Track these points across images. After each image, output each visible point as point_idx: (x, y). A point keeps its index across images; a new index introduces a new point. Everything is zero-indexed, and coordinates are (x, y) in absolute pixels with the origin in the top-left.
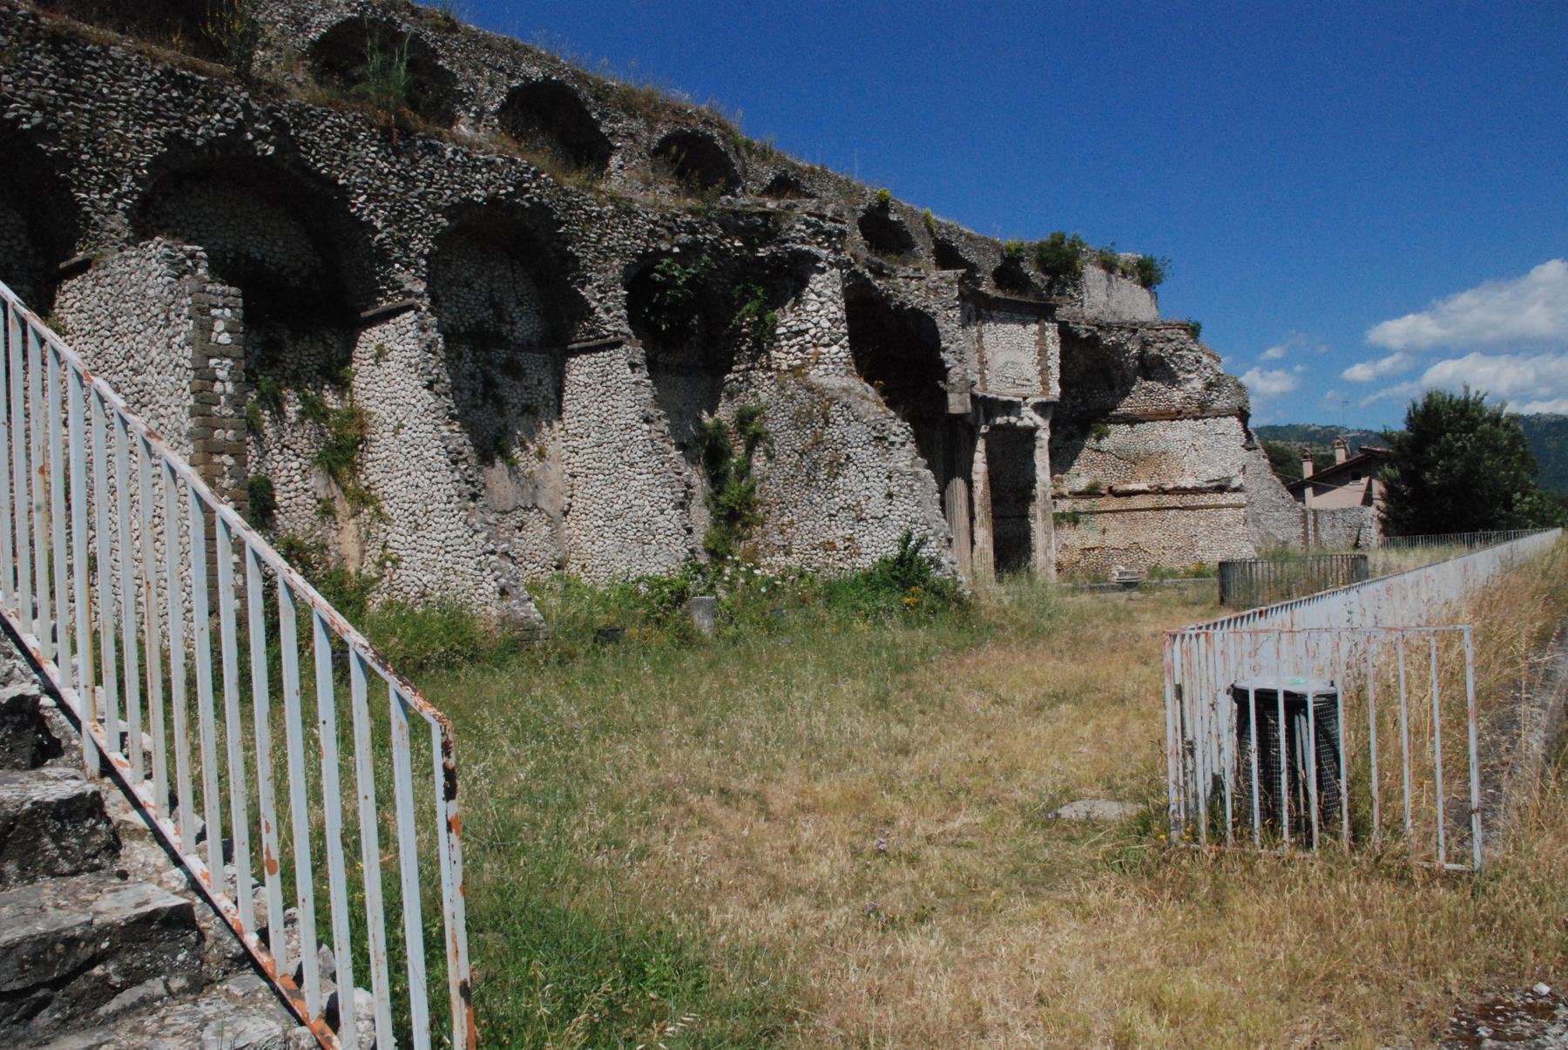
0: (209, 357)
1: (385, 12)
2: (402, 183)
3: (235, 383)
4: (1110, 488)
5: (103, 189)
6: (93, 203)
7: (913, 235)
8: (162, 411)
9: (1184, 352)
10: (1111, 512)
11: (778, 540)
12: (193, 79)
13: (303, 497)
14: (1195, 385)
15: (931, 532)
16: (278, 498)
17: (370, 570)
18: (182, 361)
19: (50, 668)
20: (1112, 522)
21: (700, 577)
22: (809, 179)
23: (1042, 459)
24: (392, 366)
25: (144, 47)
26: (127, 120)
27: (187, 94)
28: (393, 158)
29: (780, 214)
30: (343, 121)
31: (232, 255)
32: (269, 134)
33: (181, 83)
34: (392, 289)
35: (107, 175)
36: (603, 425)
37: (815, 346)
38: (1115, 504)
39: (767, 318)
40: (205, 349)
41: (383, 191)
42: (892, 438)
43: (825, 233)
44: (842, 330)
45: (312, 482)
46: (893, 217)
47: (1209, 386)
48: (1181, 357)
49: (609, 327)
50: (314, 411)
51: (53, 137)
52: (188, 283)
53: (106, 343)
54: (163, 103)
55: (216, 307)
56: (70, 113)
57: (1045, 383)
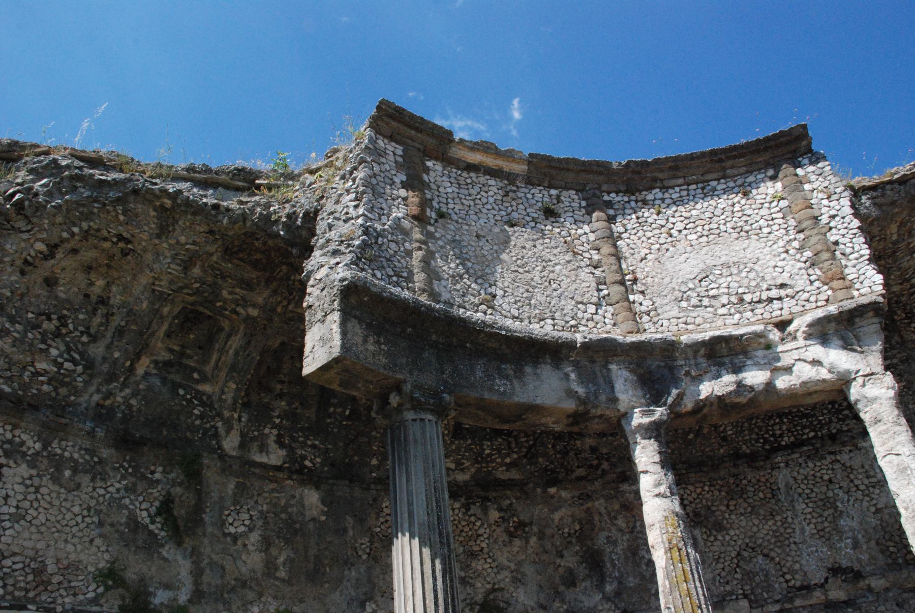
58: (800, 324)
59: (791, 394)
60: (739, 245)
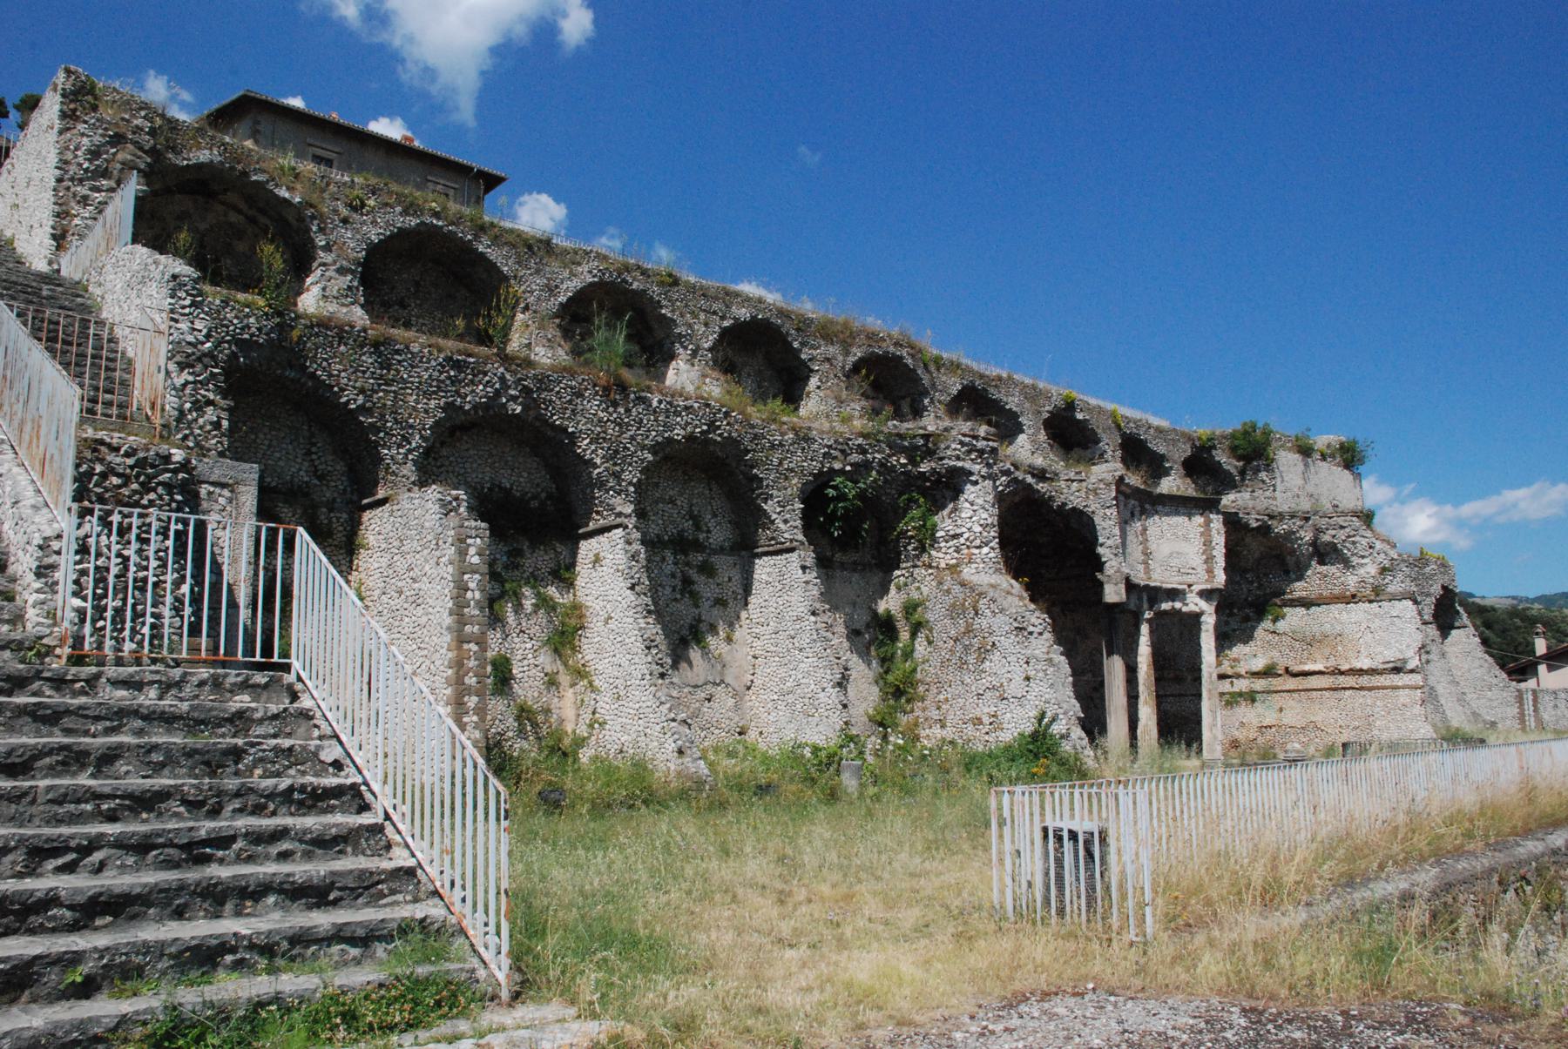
1: (619, 275)
3: (482, 591)
4: (1287, 669)
5: (400, 446)
6: (392, 458)
7: (1099, 431)
9: (1357, 539)
10: (1289, 691)
11: (935, 714)
12: (465, 361)
14: (1369, 569)
15: (1061, 711)
17: (583, 731)
19: (365, 772)
20: (1289, 702)
21: (852, 745)
22: (996, 386)
23: (1207, 641)
24: (605, 570)
25: (433, 340)
26: (418, 395)
27: (460, 372)
28: (611, 409)
29: (939, 435)
32: (517, 397)
33: (459, 366)
35: (403, 436)
36: (779, 616)
37: (968, 547)
38: (1292, 683)
39: (929, 524)
40: (463, 569)
41: (602, 435)
42: (1031, 629)
43: (977, 451)
44: (992, 534)
45: (541, 659)
46: (1080, 416)
47: (1383, 570)
48: (1354, 543)
49: (786, 535)
50: (544, 603)
51: (367, 411)
52: (453, 520)
53: (396, 558)
54: (443, 382)
57: (1210, 571)
58: (1196, 588)
59: (1185, 613)
60: (1183, 544)
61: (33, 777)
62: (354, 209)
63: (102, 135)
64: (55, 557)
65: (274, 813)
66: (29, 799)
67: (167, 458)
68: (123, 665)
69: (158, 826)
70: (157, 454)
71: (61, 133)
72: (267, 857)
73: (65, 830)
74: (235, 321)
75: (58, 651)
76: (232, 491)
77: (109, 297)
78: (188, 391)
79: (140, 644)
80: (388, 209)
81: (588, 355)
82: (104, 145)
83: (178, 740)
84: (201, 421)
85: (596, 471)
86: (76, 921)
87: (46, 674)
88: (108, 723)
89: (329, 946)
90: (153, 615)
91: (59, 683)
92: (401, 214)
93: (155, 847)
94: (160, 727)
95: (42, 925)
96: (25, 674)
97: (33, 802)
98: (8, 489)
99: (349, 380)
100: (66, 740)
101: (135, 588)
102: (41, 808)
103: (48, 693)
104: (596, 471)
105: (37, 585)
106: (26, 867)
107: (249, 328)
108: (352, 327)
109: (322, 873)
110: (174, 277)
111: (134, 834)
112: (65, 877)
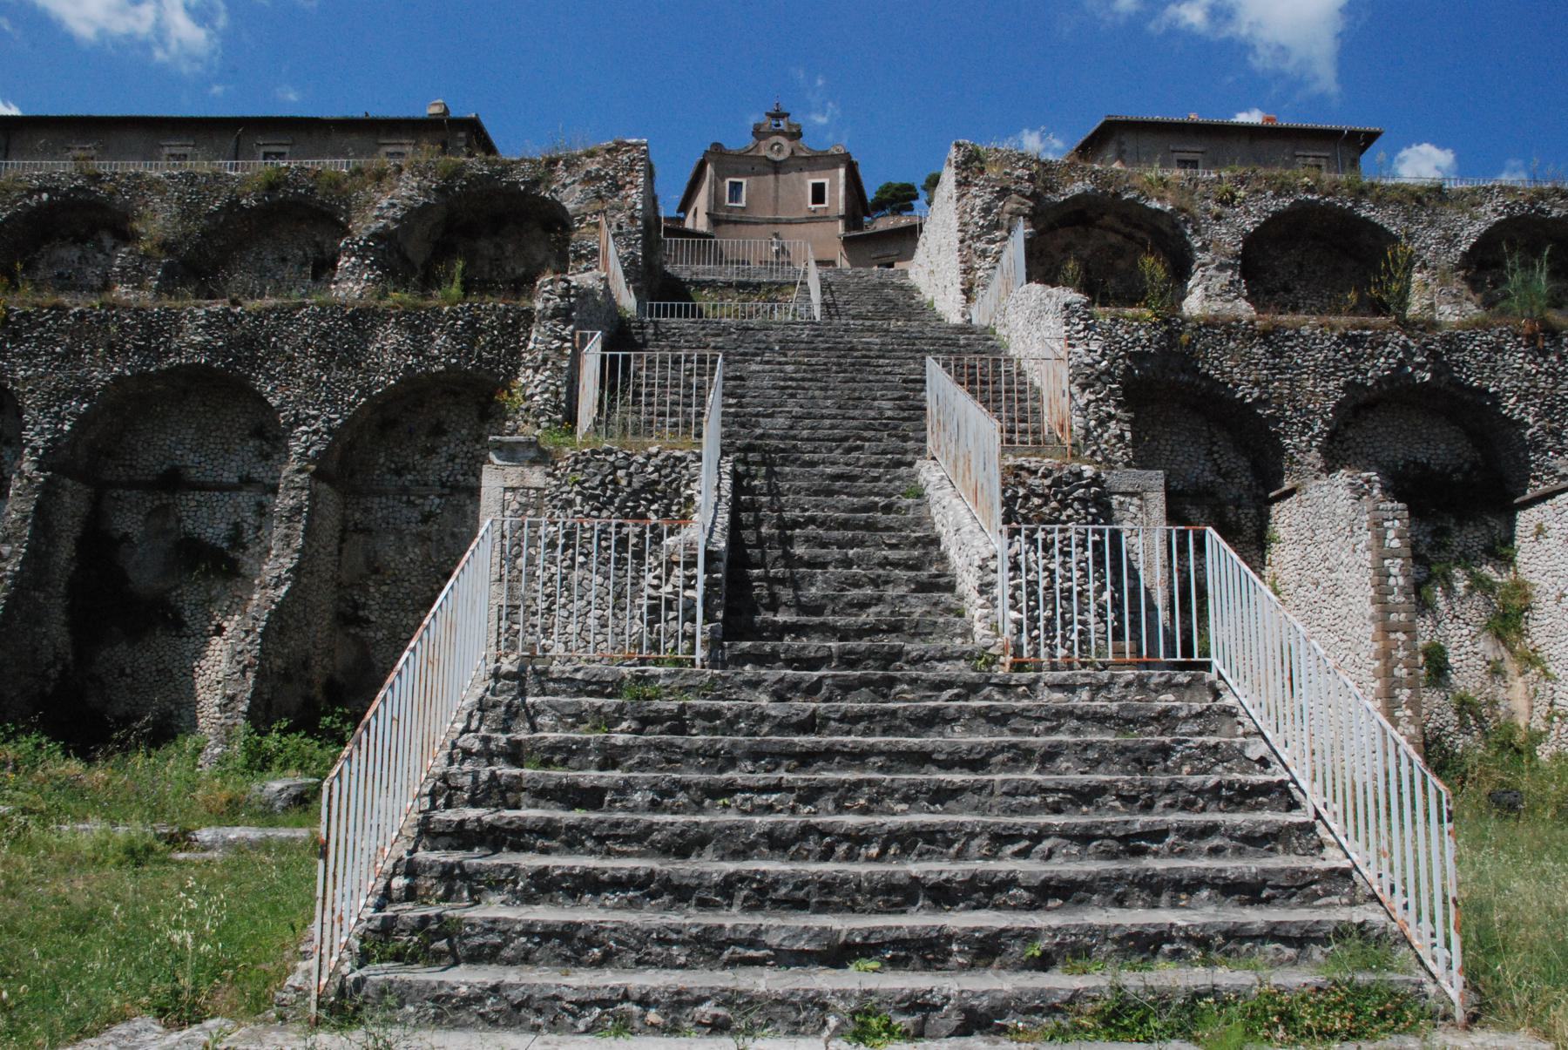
0: (1384, 559)
1: (1533, 204)
2: (1550, 380)
3: (1406, 576)
5: (1302, 434)
6: (1295, 447)
8: (1351, 600)
12: (1361, 336)
13: (1473, 659)
16: (1450, 661)
17: (1539, 724)
18: (1364, 563)
19: (1292, 769)
24: (1552, 542)
25: (1325, 319)
26: (1315, 379)
27: (1357, 348)
28: (1540, 360)
30: (1490, 337)
31: (1402, 463)
32: (1426, 364)
33: (1355, 341)
34: (1547, 474)
35: (1304, 423)
40: (1382, 553)
45: (1481, 646)
50: (1480, 585)
51: (1264, 403)
52: (1367, 503)
53: (1309, 549)
54: (1340, 361)
55: (1388, 520)
56: (1276, 384)
61: (990, 772)
62: (1225, 203)
63: (991, 193)
64: (993, 575)
65: (1203, 810)
66: (988, 790)
67: (1079, 475)
68: (1057, 670)
69: (1097, 819)
70: (1070, 472)
71: (958, 200)
72: (1199, 852)
73: (1019, 820)
74: (1126, 336)
75: (1002, 659)
76: (1141, 499)
77: (1013, 336)
78: (1091, 410)
79: (1071, 649)
80: (1260, 196)
81: (1503, 304)
82: (993, 201)
83: (1110, 739)
84: (1106, 436)
85: (1529, 432)
86: (1032, 902)
87: (994, 680)
88: (1048, 724)
89: (1263, 944)
90: (1080, 622)
91: (1005, 687)
92: (1273, 197)
93: (1095, 838)
94: (1093, 726)
95: (1005, 902)
96: (977, 681)
97: (992, 793)
98: (951, 519)
99: (1242, 375)
100: (1014, 739)
101: (1062, 598)
102: (999, 799)
103: (996, 697)
104: (1529, 432)
105: (981, 601)
106: (990, 850)
107: (1140, 340)
108: (1239, 321)
109: (1254, 870)
110: (1067, 306)
111: (1076, 825)
112: (1021, 862)
